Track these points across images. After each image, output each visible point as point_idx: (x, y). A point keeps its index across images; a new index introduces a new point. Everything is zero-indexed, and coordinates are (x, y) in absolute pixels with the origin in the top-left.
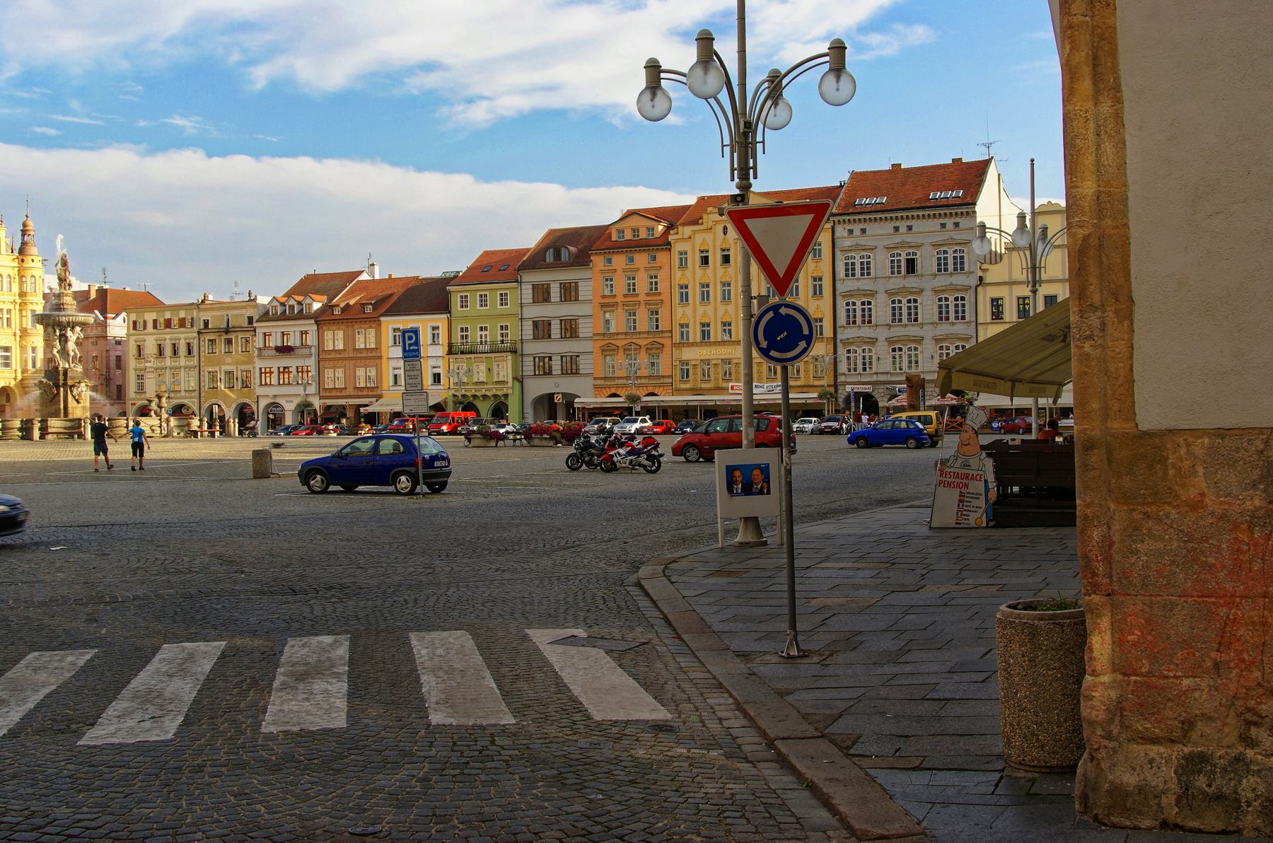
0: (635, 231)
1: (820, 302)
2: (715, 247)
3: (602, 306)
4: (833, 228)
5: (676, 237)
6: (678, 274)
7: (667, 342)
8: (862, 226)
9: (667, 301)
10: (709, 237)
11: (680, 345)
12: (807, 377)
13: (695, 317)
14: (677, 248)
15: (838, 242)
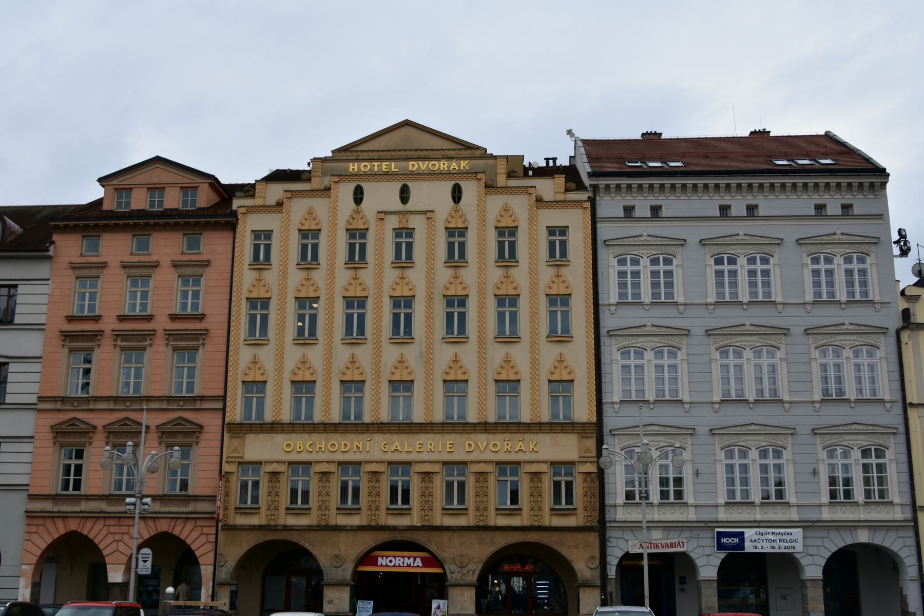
0: (156, 189)
1: (565, 349)
2: (333, 225)
3: (67, 336)
4: (592, 201)
5: (249, 202)
6: (246, 278)
7: (211, 422)
8: (653, 200)
9: (218, 333)
10: (320, 205)
11: (239, 429)
12: (536, 508)
13: (279, 369)
14: (249, 224)
15: (606, 231)
